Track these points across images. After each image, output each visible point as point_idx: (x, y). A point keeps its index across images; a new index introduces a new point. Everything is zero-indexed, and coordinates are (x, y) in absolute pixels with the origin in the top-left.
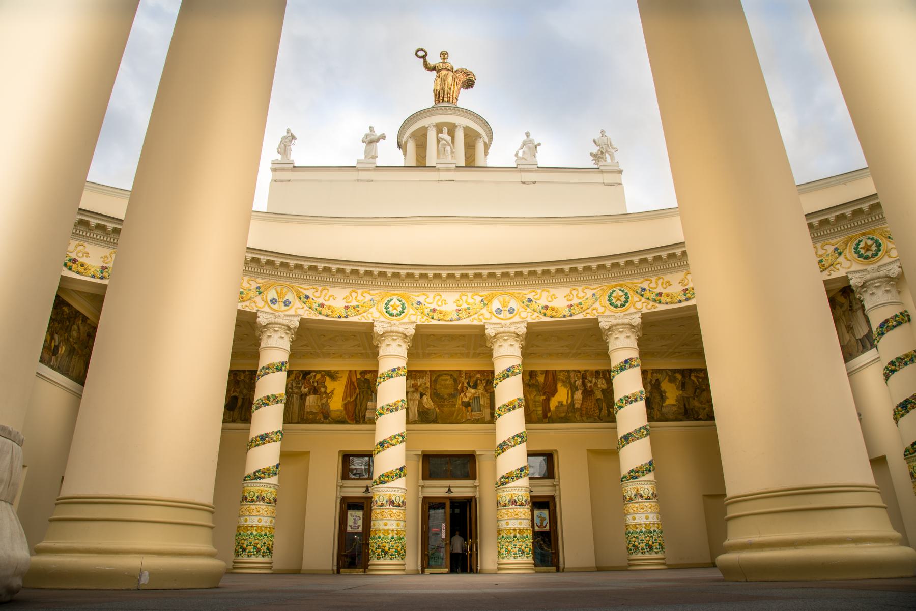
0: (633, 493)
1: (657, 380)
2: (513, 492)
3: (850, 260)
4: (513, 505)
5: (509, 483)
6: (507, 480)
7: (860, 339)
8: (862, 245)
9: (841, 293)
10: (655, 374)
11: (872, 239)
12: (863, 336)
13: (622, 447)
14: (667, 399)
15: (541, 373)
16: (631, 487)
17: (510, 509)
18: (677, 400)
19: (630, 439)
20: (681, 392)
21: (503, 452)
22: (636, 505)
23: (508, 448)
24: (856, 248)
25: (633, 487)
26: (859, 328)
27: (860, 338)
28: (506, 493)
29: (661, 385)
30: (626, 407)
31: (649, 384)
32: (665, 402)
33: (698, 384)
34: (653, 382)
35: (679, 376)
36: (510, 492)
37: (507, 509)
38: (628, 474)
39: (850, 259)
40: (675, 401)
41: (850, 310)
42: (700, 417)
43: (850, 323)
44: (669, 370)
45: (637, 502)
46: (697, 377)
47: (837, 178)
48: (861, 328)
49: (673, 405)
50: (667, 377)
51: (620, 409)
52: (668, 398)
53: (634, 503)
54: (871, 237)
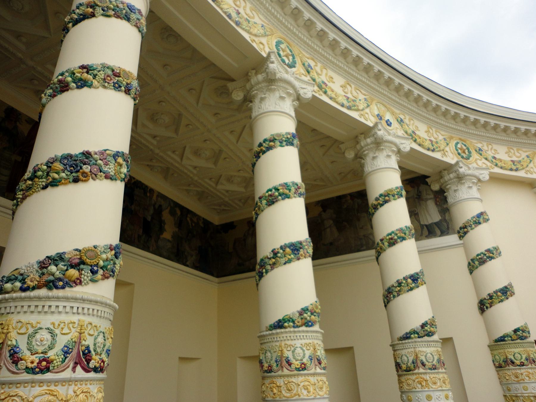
0: (308, 353)
1: (160, 206)
2: (86, 319)
3: (453, 154)
4: (79, 368)
5: (78, 282)
6: (73, 273)
7: (426, 226)
8: (459, 146)
9: (407, 182)
10: (159, 199)
11: (465, 146)
12: (432, 223)
13: (285, 264)
14: (165, 232)
15: (26, 121)
16: (303, 342)
17: (63, 382)
18: (172, 237)
19: (301, 252)
20: (177, 230)
21: (76, 180)
22: (312, 379)
23: (95, 176)
24: (456, 146)
25: (308, 341)
26: (428, 216)
27: (427, 223)
28: (56, 318)
29: (163, 213)
30: (294, 199)
31: (152, 207)
32: (162, 234)
33: (191, 227)
34: (157, 206)
35: (178, 212)
36: (75, 318)
37: (49, 382)
38: (298, 314)
39: (453, 152)
40: (171, 237)
41: (416, 198)
42: (188, 263)
43: (416, 209)
44: (172, 200)
45: (314, 375)
46: (191, 220)
47: (444, 89)
48: (430, 215)
49: (169, 241)
50: (169, 208)
51: (283, 199)
52: (166, 231)
53: (308, 375)
54: (464, 143)
